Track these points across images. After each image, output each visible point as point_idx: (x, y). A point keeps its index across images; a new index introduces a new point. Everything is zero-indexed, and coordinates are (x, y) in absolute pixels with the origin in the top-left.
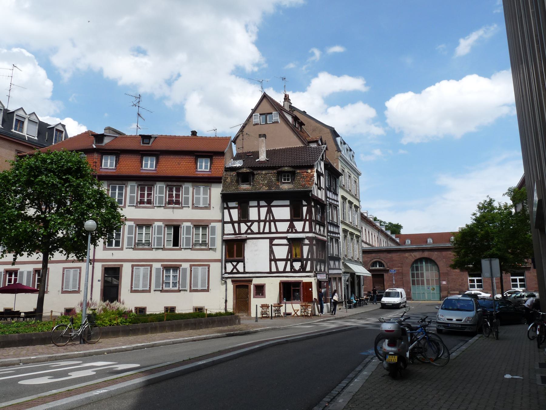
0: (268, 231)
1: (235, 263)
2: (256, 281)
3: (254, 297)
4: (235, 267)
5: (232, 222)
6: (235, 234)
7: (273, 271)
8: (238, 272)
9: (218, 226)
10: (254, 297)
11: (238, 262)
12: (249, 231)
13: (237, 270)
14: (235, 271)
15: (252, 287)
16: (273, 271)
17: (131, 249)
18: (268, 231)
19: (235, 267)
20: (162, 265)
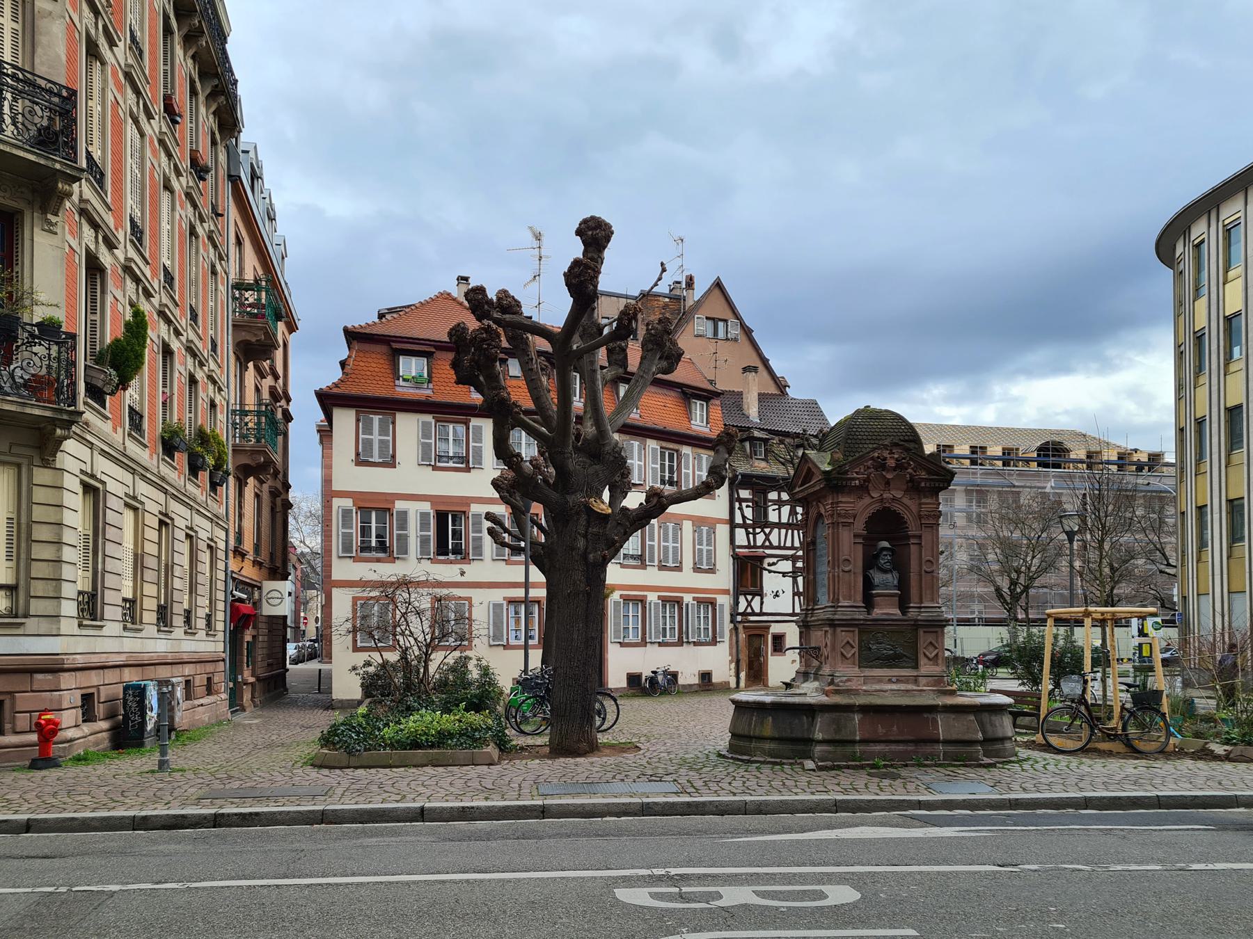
0: (790, 545)
1: (749, 597)
2: (775, 629)
3: (772, 655)
4: (749, 604)
5: (744, 526)
6: (748, 547)
7: (796, 611)
8: (753, 614)
9: (723, 531)
10: (772, 655)
11: (754, 595)
12: (767, 543)
13: (752, 609)
14: (749, 610)
15: (770, 637)
16: (796, 611)
17: (348, 560)
18: (790, 545)
19: (749, 604)
20: (659, 597)
